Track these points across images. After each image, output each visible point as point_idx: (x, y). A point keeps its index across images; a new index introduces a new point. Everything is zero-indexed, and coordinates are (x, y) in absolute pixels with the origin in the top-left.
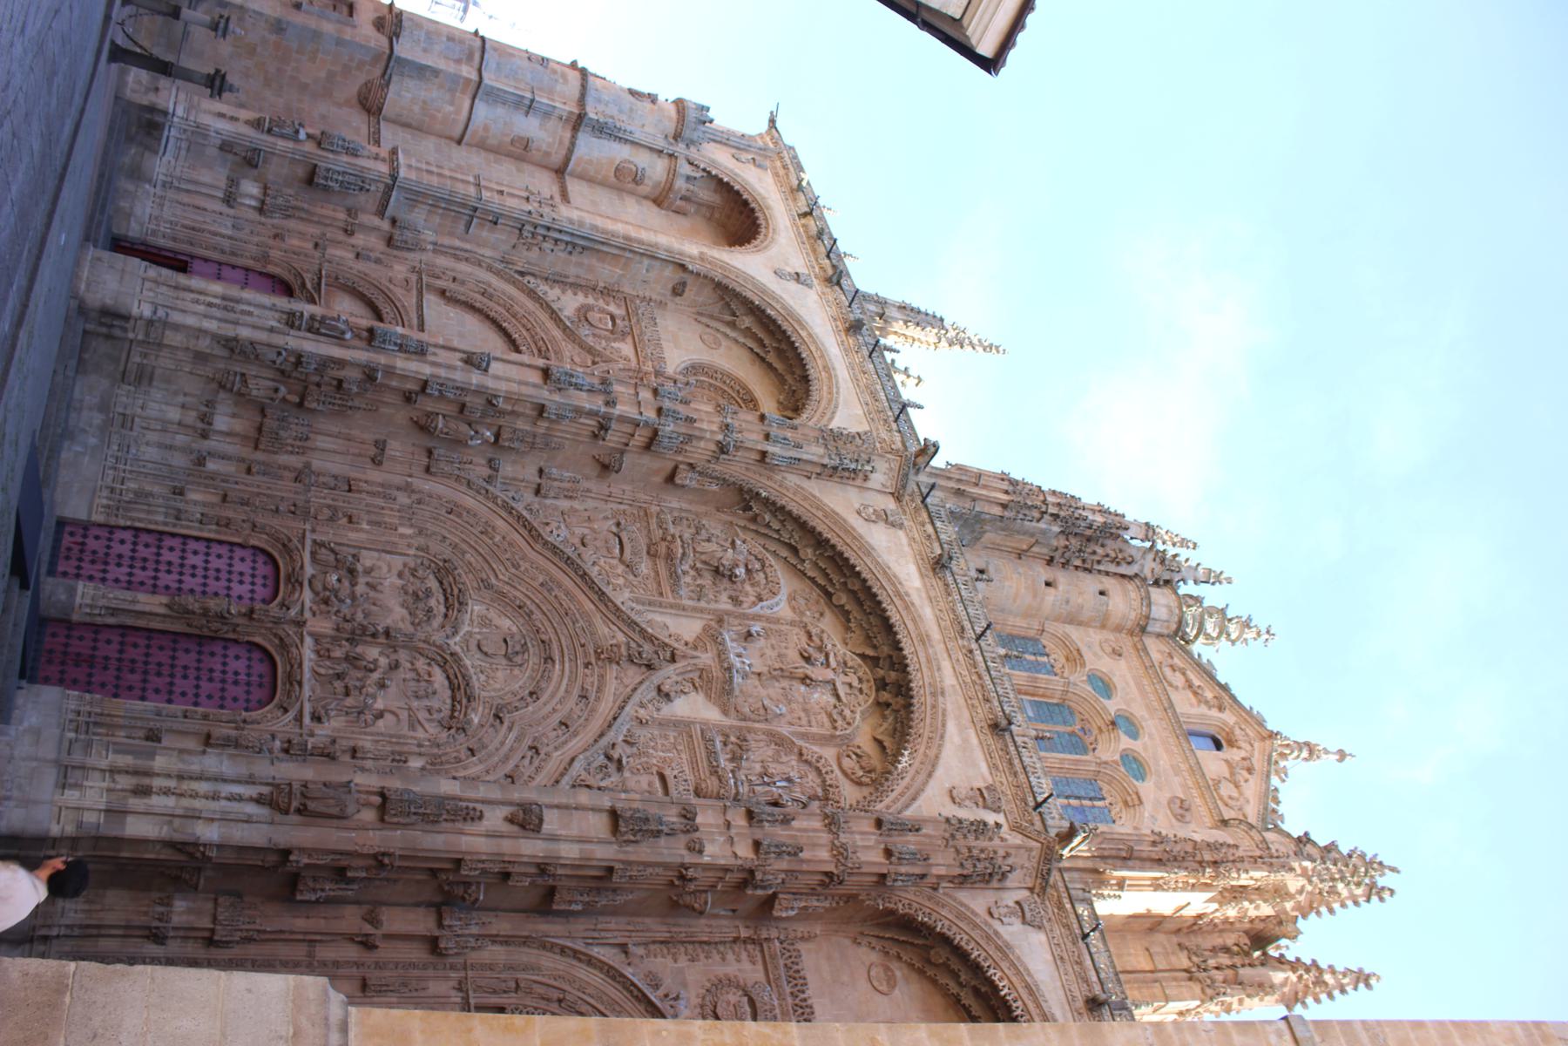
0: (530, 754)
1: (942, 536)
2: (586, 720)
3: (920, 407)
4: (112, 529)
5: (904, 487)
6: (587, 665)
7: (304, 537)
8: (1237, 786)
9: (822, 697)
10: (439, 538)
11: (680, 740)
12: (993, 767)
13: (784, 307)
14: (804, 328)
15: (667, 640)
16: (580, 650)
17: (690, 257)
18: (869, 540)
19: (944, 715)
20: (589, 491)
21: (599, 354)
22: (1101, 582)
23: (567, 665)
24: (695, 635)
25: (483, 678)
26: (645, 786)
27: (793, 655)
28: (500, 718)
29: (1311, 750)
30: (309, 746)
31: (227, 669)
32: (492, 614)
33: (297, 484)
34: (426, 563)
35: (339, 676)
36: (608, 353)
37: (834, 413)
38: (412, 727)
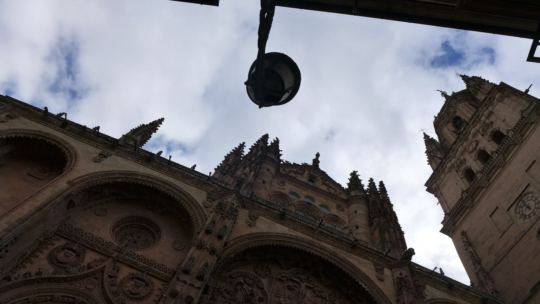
1: (265, 204)
3: (195, 166)
5: (243, 202)
8: (331, 187)
9: (309, 293)
12: (365, 258)
13: (122, 174)
14: (137, 175)
17: (68, 189)
18: (265, 231)
19: (345, 259)
21: (94, 273)
22: (265, 168)
27: (288, 293)
29: (316, 161)
36: (97, 268)
37: (193, 198)
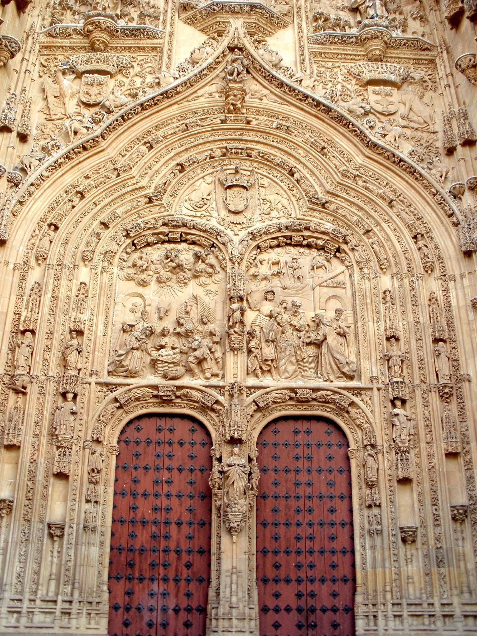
0: (360, 183)
2: (313, 131)
4: (114, 608)
6: (248, 122)
7: (107, 385)
10: (95, 240)
11: (323, 63)
15: (221, 49)
16: (229, 125)
20: (24, 89)
23: (249, 138)
24: (198, 33)
25: (274, 214)
26: (379, 98)
28: (327, 202)
30: (400, 380)
31: (292, 468)
32: (196, 197)
33: (28, 390)
34: (125, 257)
35: (296, 353)
38: (341, 285)
